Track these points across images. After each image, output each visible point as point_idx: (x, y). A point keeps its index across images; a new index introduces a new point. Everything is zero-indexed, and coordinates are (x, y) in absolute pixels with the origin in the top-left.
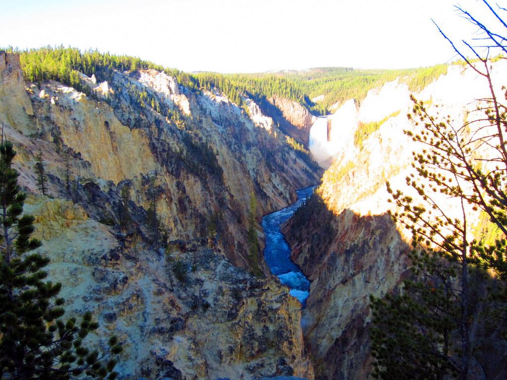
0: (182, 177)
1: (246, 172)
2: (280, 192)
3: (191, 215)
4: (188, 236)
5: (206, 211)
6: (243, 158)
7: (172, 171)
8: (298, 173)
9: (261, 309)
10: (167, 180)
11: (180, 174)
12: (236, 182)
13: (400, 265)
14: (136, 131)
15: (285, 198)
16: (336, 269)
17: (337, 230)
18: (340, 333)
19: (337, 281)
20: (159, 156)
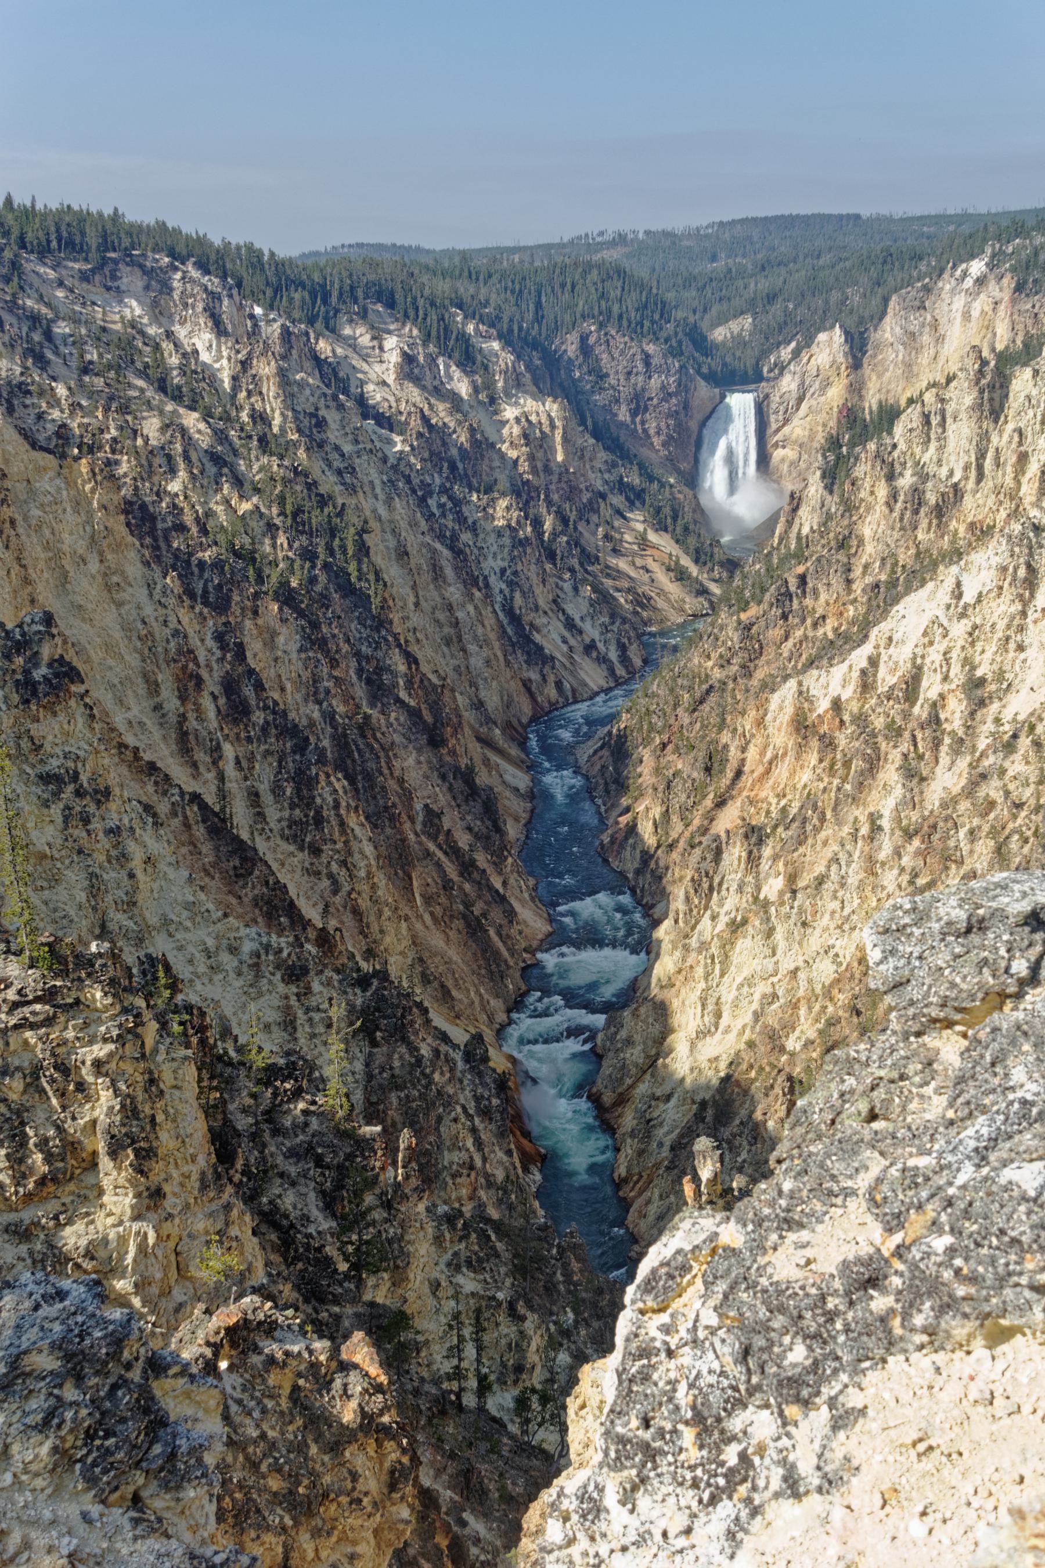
0: (235, 609)
1: (473, 581)
2: (587, 641)
3: (265, 730)
4: (257, 795)
5: (316, 715)
6: (466, 537)
7: (205, 591)
10: (185, 621)
11: (228, 600)
12: (441, 616)
13: (902, 870)
15: (603, 660)
16: (720, 884)
20: (163, 545)
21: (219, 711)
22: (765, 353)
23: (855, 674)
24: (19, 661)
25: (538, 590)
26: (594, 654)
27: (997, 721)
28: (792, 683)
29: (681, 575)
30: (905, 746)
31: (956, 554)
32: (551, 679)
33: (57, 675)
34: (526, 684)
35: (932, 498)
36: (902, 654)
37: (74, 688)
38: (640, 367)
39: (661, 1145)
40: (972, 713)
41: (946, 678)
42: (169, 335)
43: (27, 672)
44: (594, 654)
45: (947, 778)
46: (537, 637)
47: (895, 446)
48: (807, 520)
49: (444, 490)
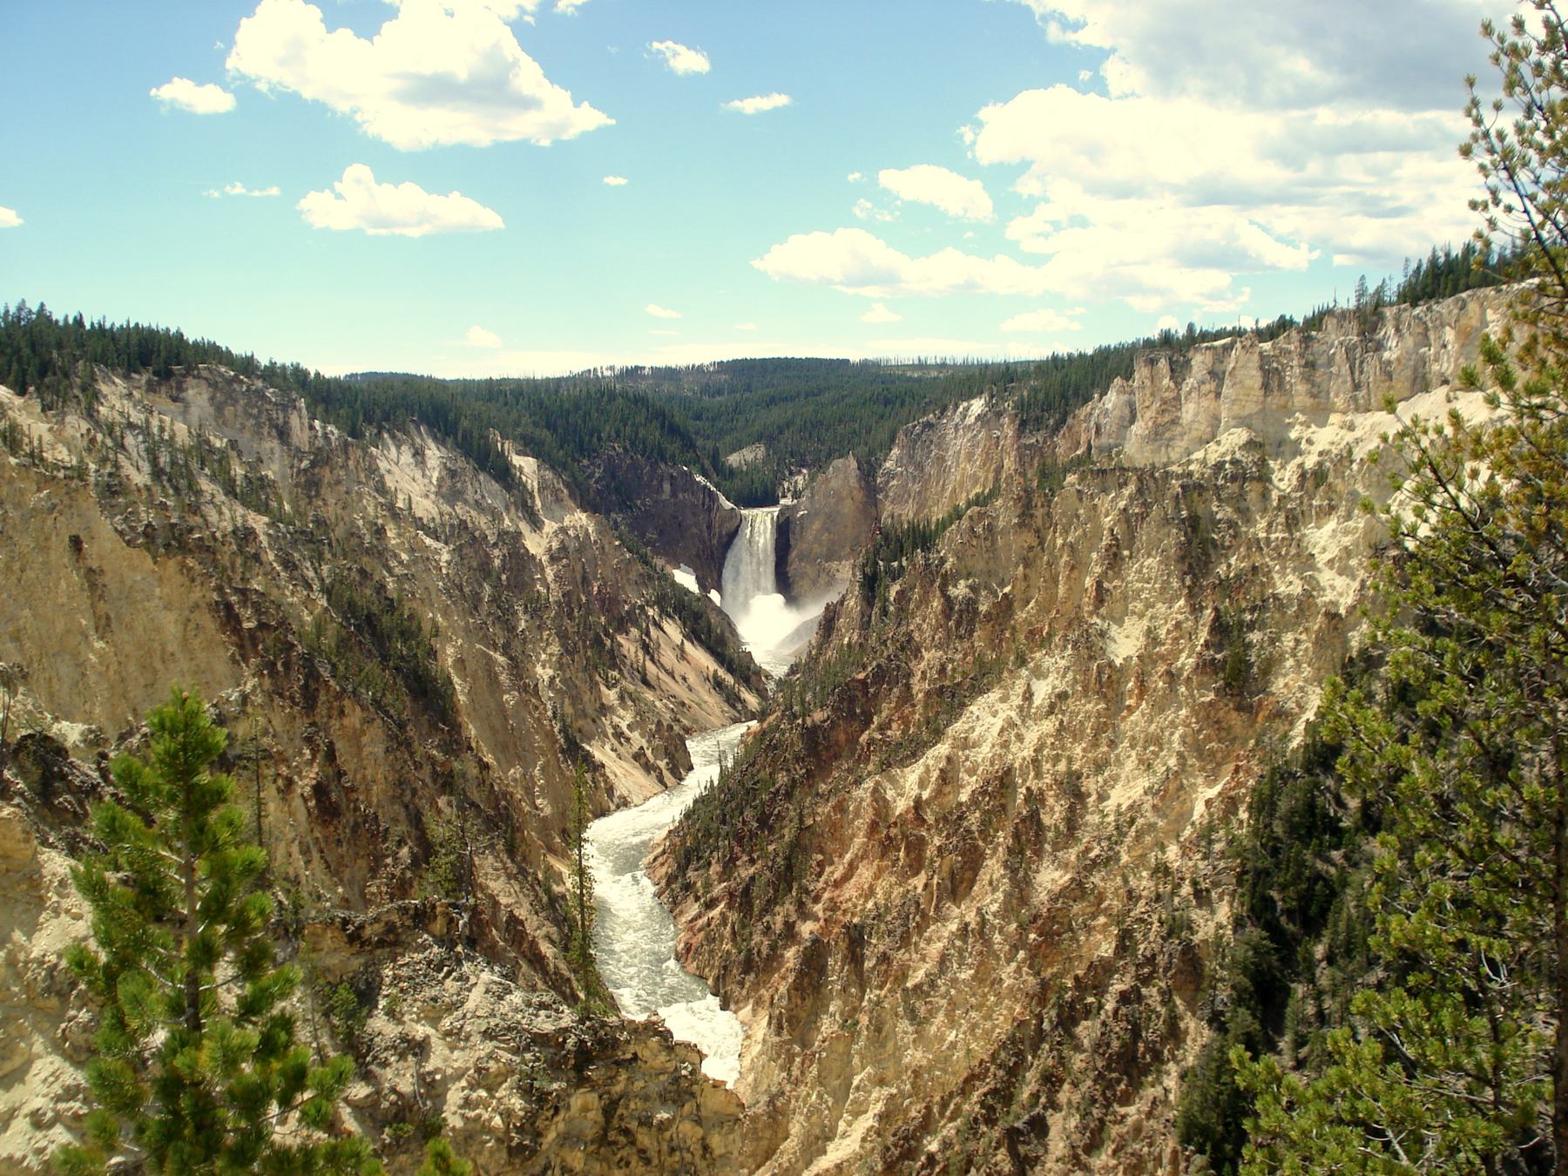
2: (635, 749)
5: (403, 816)
9: (615, 1122)
14: (172, 565)
21: (309, 813)
22: (777, 480)
23: (935, 774)
25: (586, 697)
26: (643, 760)
28: (869, 784)
29: (718, 684)
31: (1022, 661)
35: (983, 608)
38: (667, 486)
40: (1071, 809)
41: (1038, 775)
44: (643, 760)
47: (943, 561)
49: (494, 600)
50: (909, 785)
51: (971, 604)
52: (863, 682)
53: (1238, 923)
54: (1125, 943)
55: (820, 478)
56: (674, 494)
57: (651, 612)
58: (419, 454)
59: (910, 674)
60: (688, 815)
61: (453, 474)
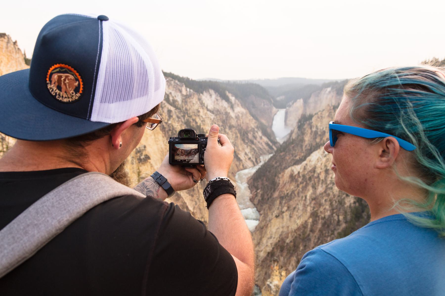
8: (262, 146)
13: (311, 207)
15: (252, 161)
17: (279, 183)
18: (271, 249)
19: (274, 215)
23: (303, 167)
24: (139, 154)
27: (332, 178)
30: (313, 182)
32: (241, 164)
33: (146, 158)
34: (236, 165)
35: (319, 133)
36: (313, 163)
37: (149, 161)
38: (263, 104)
39: (259, 261)
42: (171, 93)
43: (140, 157)
45: (320, 189)
46: (239, 156)
47: (312, 123)
48: (294, 136)
49: (222, 126)
50: (297, 169)
51: (316, 133)
52: (293, 147)
53: (355, 203)
54: (331, 204)
55: (295, 104)
56: (264, 105)
57: (256, 129)
58: (211, 95)
59: (302, 146)
60: (257, 172)
61: (217, 100)
